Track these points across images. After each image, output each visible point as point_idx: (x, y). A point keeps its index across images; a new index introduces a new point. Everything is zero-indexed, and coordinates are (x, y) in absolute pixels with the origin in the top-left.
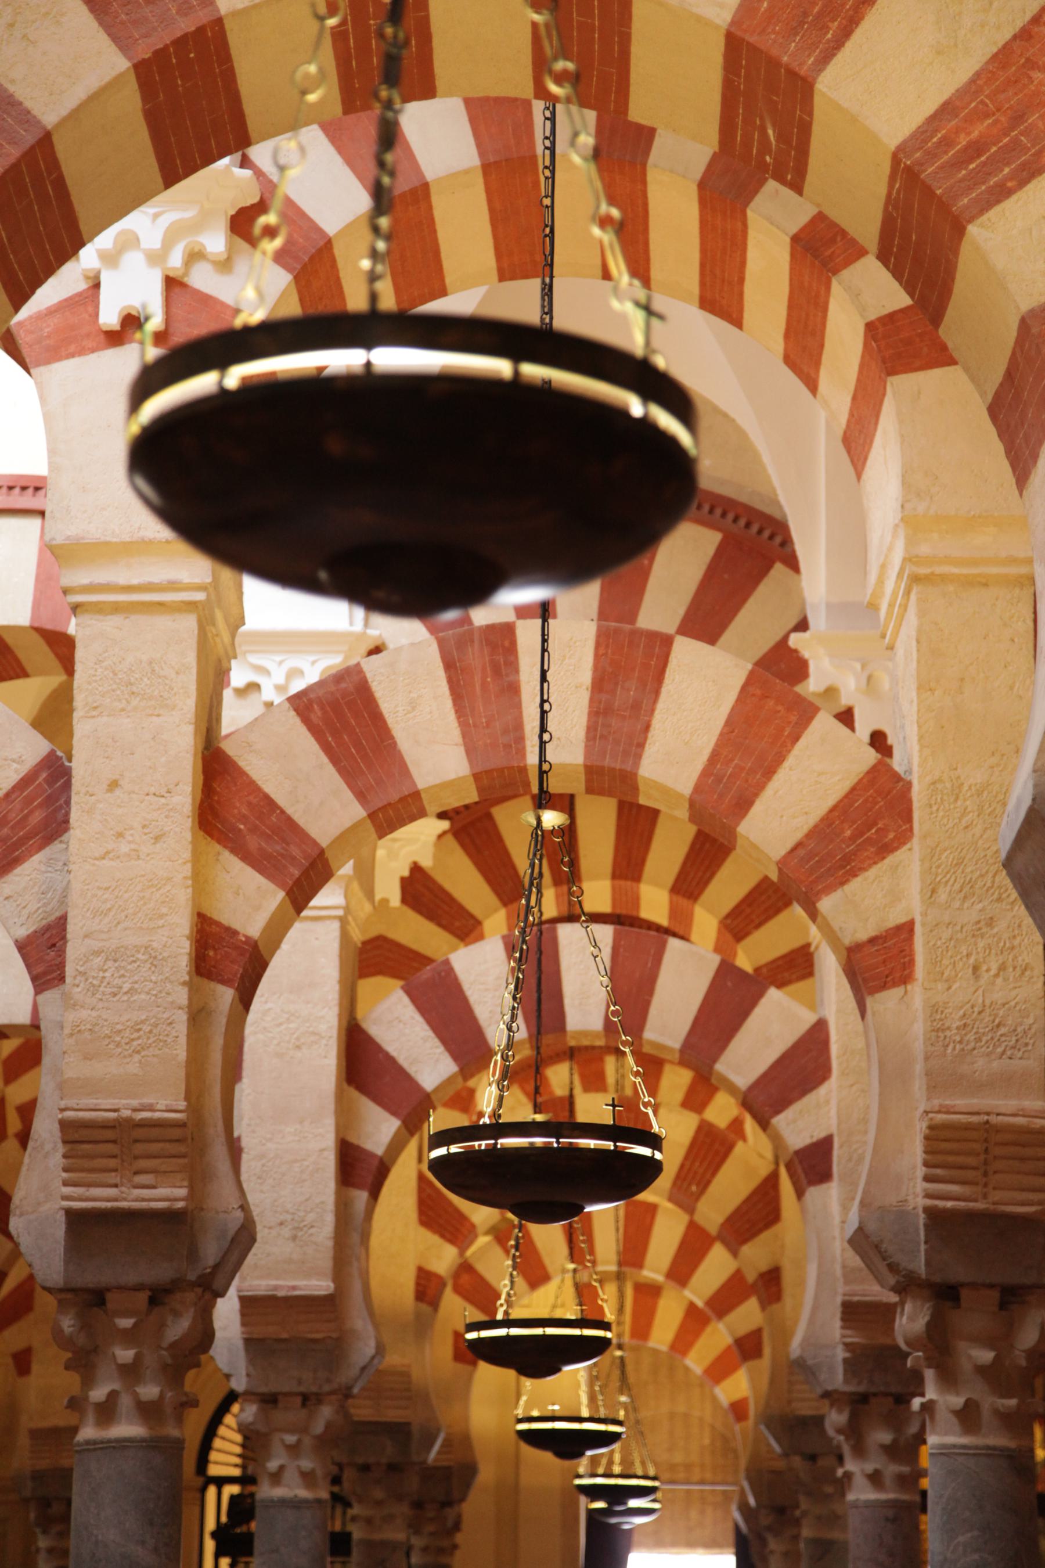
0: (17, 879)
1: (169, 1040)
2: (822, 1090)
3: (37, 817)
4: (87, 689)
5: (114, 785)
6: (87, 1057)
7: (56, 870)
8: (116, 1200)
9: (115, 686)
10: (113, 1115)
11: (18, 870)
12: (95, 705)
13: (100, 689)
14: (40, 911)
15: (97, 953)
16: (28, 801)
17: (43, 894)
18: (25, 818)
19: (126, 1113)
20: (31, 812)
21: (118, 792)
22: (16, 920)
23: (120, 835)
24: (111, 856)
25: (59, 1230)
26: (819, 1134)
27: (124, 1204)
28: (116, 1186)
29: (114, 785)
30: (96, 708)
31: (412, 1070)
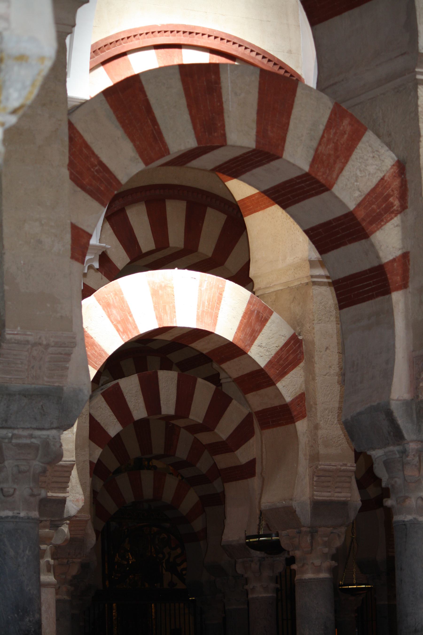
0: (286, 379)
1: (349, 442)
2: (251, 441)
3: (291, 357)
4: (317, 313)
5: (327, 348)
7: (298, 377)
8: (330, 497)
9: (326, 313)
10: (334, 467)
11: (286, 377)
12: (320, 319)
13: (321, 313)
14: (294, 392)
16: (288, 351)
17: (294, 386)
18: (288, 357)
19: (339, 467)
20: (289, 355)
21: (328, 351)
22: (287, 395)
23: (330, 367)
24: (328, 374)
26: (251, 458)
27: (333, 498)
28: (330, 492)
29: (327, 348)
30: (320, 320)
31: (106, 428)
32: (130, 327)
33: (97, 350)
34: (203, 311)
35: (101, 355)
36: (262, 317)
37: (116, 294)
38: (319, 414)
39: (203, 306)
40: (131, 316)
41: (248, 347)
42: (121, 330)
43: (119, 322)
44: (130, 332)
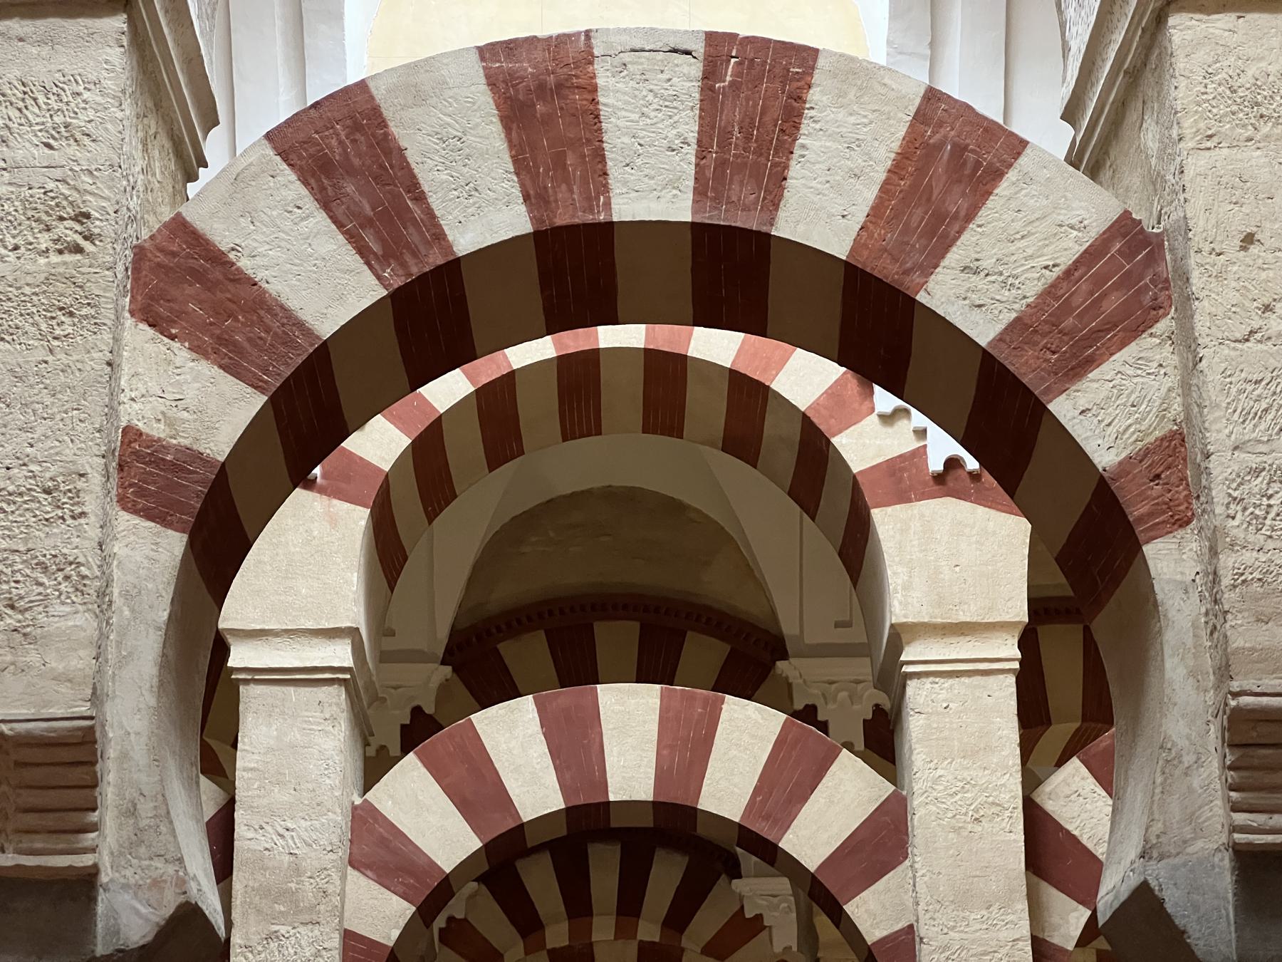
0: (1095, 385)
3: (1113, 302)
4: (1196, 112)
5: (1249, 240)
6: (1261, 619)
7: (1149, 374)
9: (1235, 108)
12: (1210, 132)
13: (1215, 111)
14: (1132, 430)
15: (1257, 472)
16: (1099, 280)
17: (1133, 406)
20: (1104, 295)
21: (1254, 249)
22: (1100, 442)
24: (1258, 336)
25: (1225, 881)
30: (1210, 137)
32: (412, 236)
33: (275, 325)
34: (721, 164)
35: (288, 342)
36: (978, 164)
37: (356, 127)
38: (1219, 494)
39: (724, 144)
40: (420, 198)
41: (916, 278)
42: (375, 247)
43: (367, 223)
44: (415, 254)
